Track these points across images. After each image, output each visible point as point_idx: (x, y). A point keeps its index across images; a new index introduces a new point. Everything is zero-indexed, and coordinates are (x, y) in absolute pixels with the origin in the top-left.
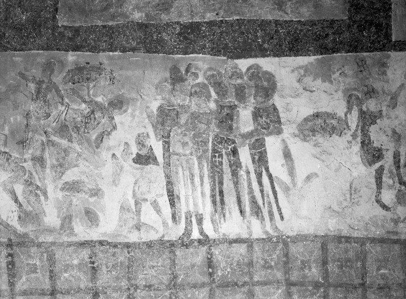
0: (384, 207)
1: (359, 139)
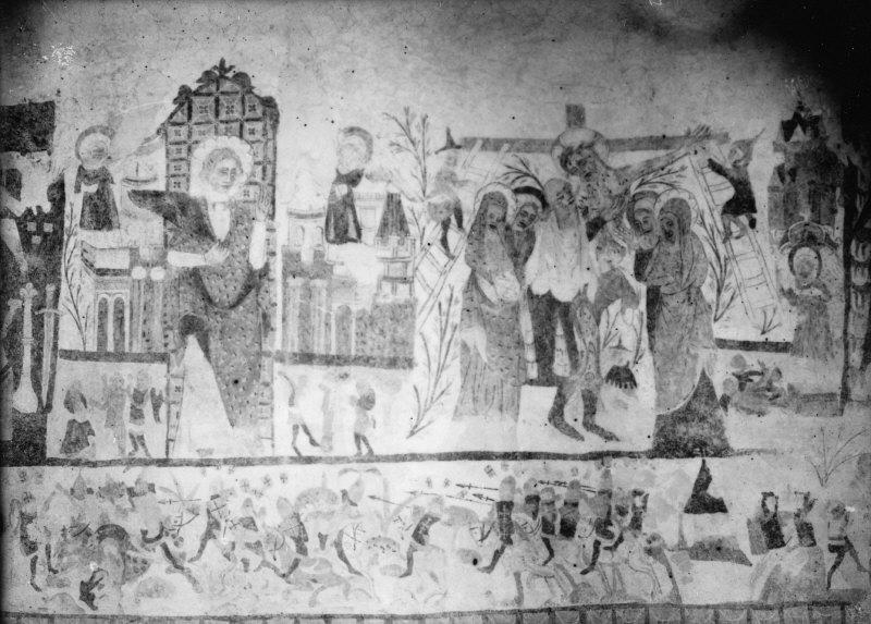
0: (37, 589)
1: (19, 535)
